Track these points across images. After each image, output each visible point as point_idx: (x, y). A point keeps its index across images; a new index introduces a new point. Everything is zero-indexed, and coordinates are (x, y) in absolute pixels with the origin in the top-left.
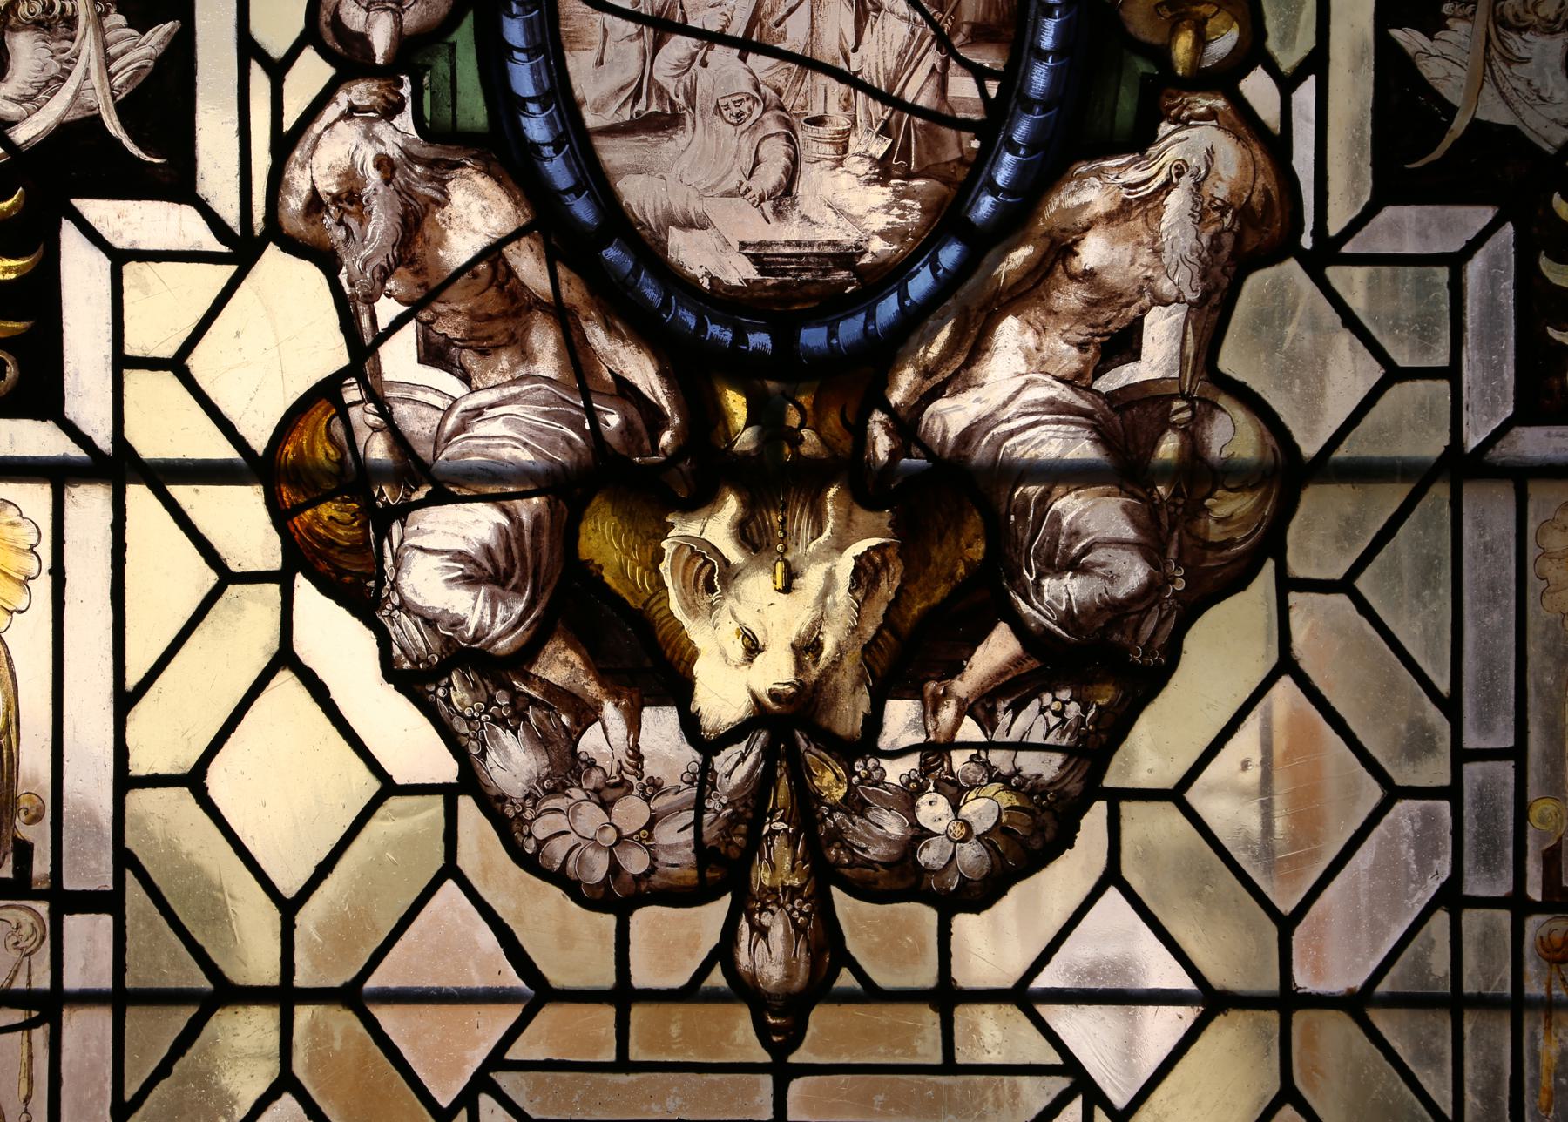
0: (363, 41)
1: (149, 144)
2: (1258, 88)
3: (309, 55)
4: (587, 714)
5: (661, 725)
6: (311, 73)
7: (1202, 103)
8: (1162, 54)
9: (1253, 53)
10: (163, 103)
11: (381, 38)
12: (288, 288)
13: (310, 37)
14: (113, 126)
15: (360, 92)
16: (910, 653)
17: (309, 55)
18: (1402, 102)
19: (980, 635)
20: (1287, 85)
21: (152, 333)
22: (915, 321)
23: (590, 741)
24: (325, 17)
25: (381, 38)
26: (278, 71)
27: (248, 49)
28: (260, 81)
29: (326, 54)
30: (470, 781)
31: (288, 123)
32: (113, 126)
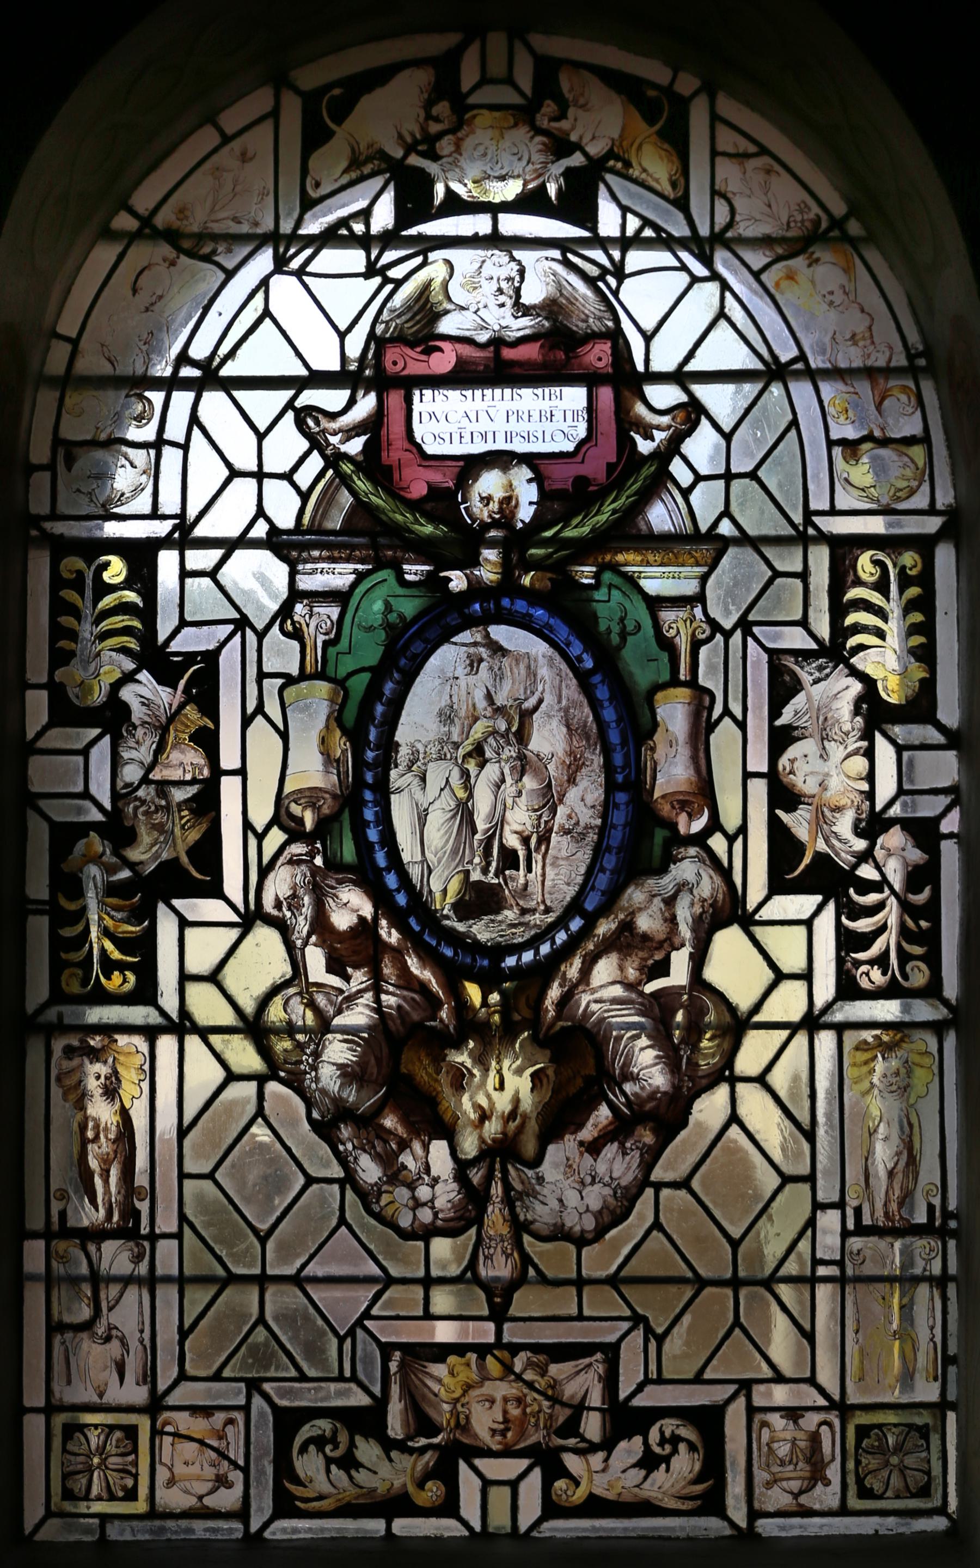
0: (300, 821)
1: (199, 872)
2: (718, 843)
3: (275, 830)
4: (404, 1145)
5: (439, 1149)
6: (276, 837)
7: (692, 851)
8: (673, 826)
9: (715, 825)
10: (208, 851)
11: (309, 820)
12: (265, 938)
13: (275, 821)
14: (185, 859)
15: (298, 849)
16: (559, 1117)
17: (275, 830)
18: (783, 845)
19: (594, 1107)
20: (731, 839)
21: (199, 962)
22: (562, 954)
23: (406, 1159)
24: (283, 811)
25: (309, 820)
26: (260, 837)
27: (247, 825)
28: (252, 842)
29: (283, 828)
30: (350, 1179)
31: (266, 859)
32: (185, 859)
